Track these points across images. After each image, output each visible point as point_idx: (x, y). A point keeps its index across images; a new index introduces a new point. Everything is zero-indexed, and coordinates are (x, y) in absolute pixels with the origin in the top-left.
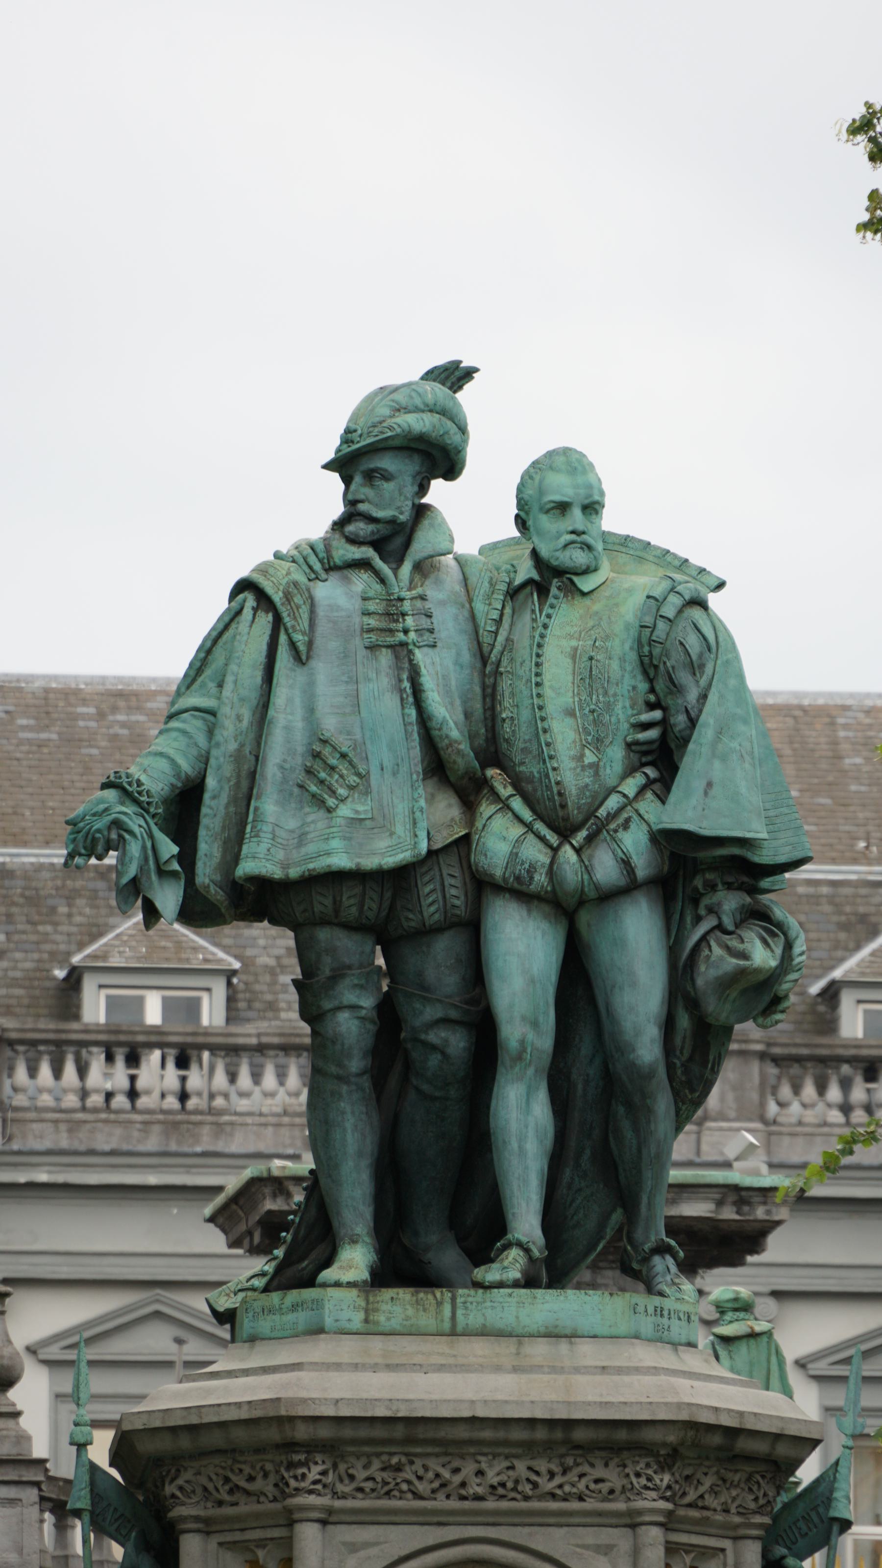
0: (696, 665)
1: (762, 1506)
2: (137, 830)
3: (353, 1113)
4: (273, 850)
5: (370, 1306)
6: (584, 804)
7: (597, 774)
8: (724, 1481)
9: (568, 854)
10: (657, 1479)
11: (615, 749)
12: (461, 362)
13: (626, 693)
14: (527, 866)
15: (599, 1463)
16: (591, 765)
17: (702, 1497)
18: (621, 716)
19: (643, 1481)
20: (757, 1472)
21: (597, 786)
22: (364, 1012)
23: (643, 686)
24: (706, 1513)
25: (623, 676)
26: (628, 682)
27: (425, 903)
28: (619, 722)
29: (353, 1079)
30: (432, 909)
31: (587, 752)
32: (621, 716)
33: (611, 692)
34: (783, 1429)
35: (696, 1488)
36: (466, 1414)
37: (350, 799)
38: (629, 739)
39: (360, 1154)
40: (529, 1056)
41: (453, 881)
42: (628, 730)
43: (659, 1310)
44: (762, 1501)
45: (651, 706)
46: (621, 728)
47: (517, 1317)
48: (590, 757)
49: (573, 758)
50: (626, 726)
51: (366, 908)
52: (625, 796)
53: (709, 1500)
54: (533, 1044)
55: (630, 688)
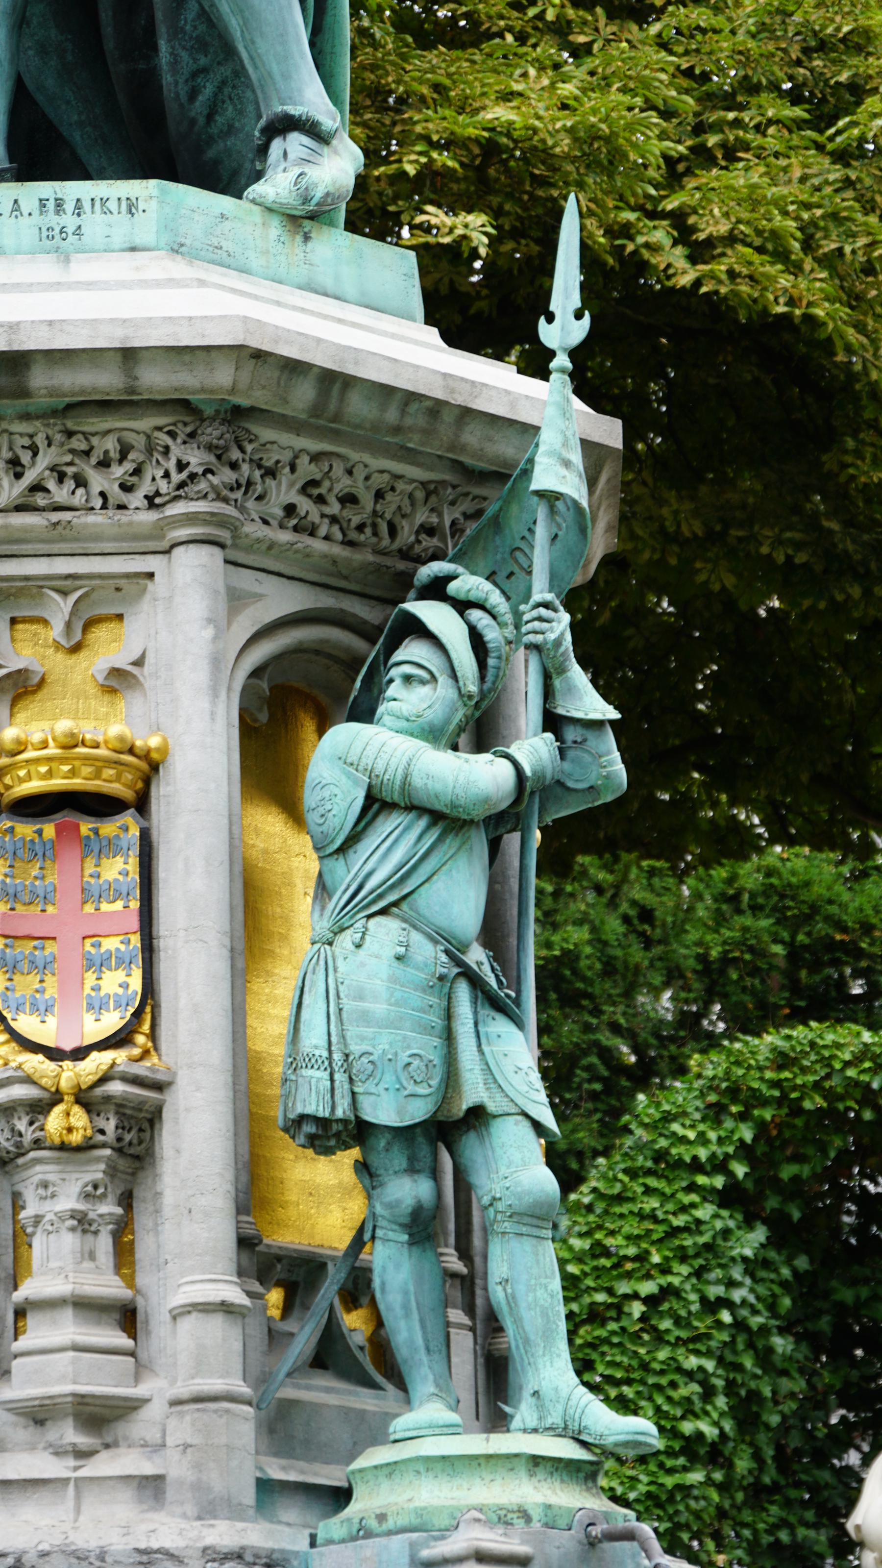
1: (181, 485)
17: (37, 488)
20: (159, 429)
24: (55, 517)
35: (18, 476)
43: (51, 205)
44: (176, 478)
53: (61, 494)
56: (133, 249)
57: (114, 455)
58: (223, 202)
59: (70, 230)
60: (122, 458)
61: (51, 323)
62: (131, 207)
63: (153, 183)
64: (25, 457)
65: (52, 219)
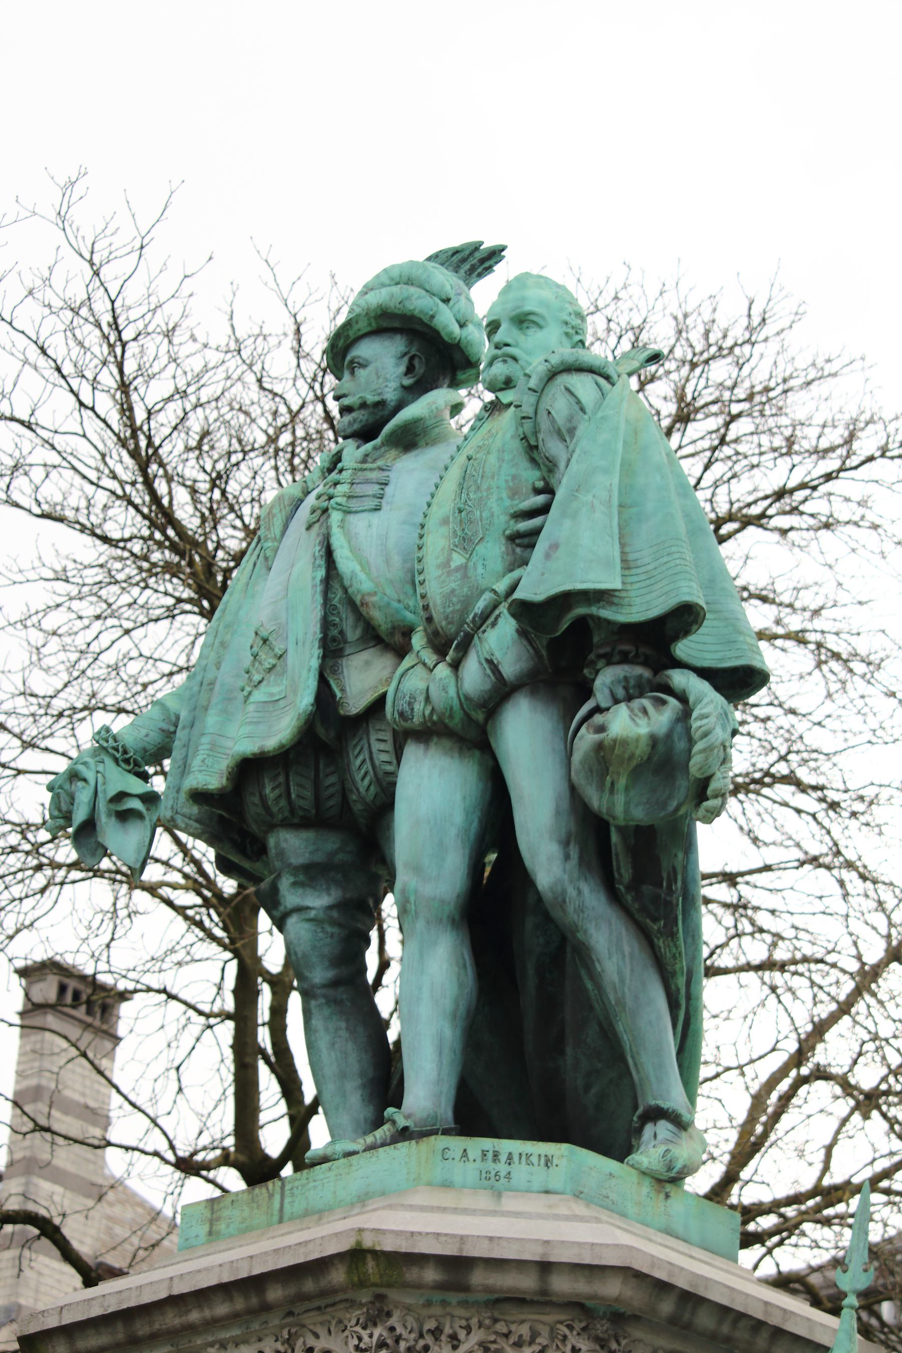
0: (564, 431)
2: (90, 775)
3: (326, 1029)
4: (209, 761)
5: (215, 1216)
6: (453, 612)
7: (465, 576)
8: (506, 1336)
9: (443, 671)
10: (365, 1334)
11: (489, 545)
12: (481, 243)
13: (503, 484)
14: (407, 698)
15: (322, 1332)
16: (457, 569)
18: (496, 510)
19: (356, 1342)
20: (561, 1323)
21: (465, 590)
22: (312, 914)
23: (531, 476)
25: (500, 467)
26: (506, 471)
27: (358, 777)
28: (492, 515)
29: (319, 992)
30: (366, 782)
31: (455, 556)
32: (496, 510)
33: (484, 486)
34: (544, 1254)
36: (163, 1295)
37: (264, 683)
38: (508, 532)
39: (343, 1076)
40: (413, 907)
41: (382, 746)
42: (507, 523)
43: (490, 1155)
45: (538, 492)
46: (496, 521)
47: (335, 1193)
48: (458, 560)
49: (439, 566)
50: (504, 518)
51: (293, 796)
52: (494, 592)
54: (416, 891)
55: (509, 478)
56: (547, 1192)
57: (527, 1337)
58: (609, 1164)
59: (503, 1174)
60: (532, 1342)
61: (491, 1239)
62: (548, 1162)
63: (565, 1146)
64: (462, 1334)
65: (490, 1165)
